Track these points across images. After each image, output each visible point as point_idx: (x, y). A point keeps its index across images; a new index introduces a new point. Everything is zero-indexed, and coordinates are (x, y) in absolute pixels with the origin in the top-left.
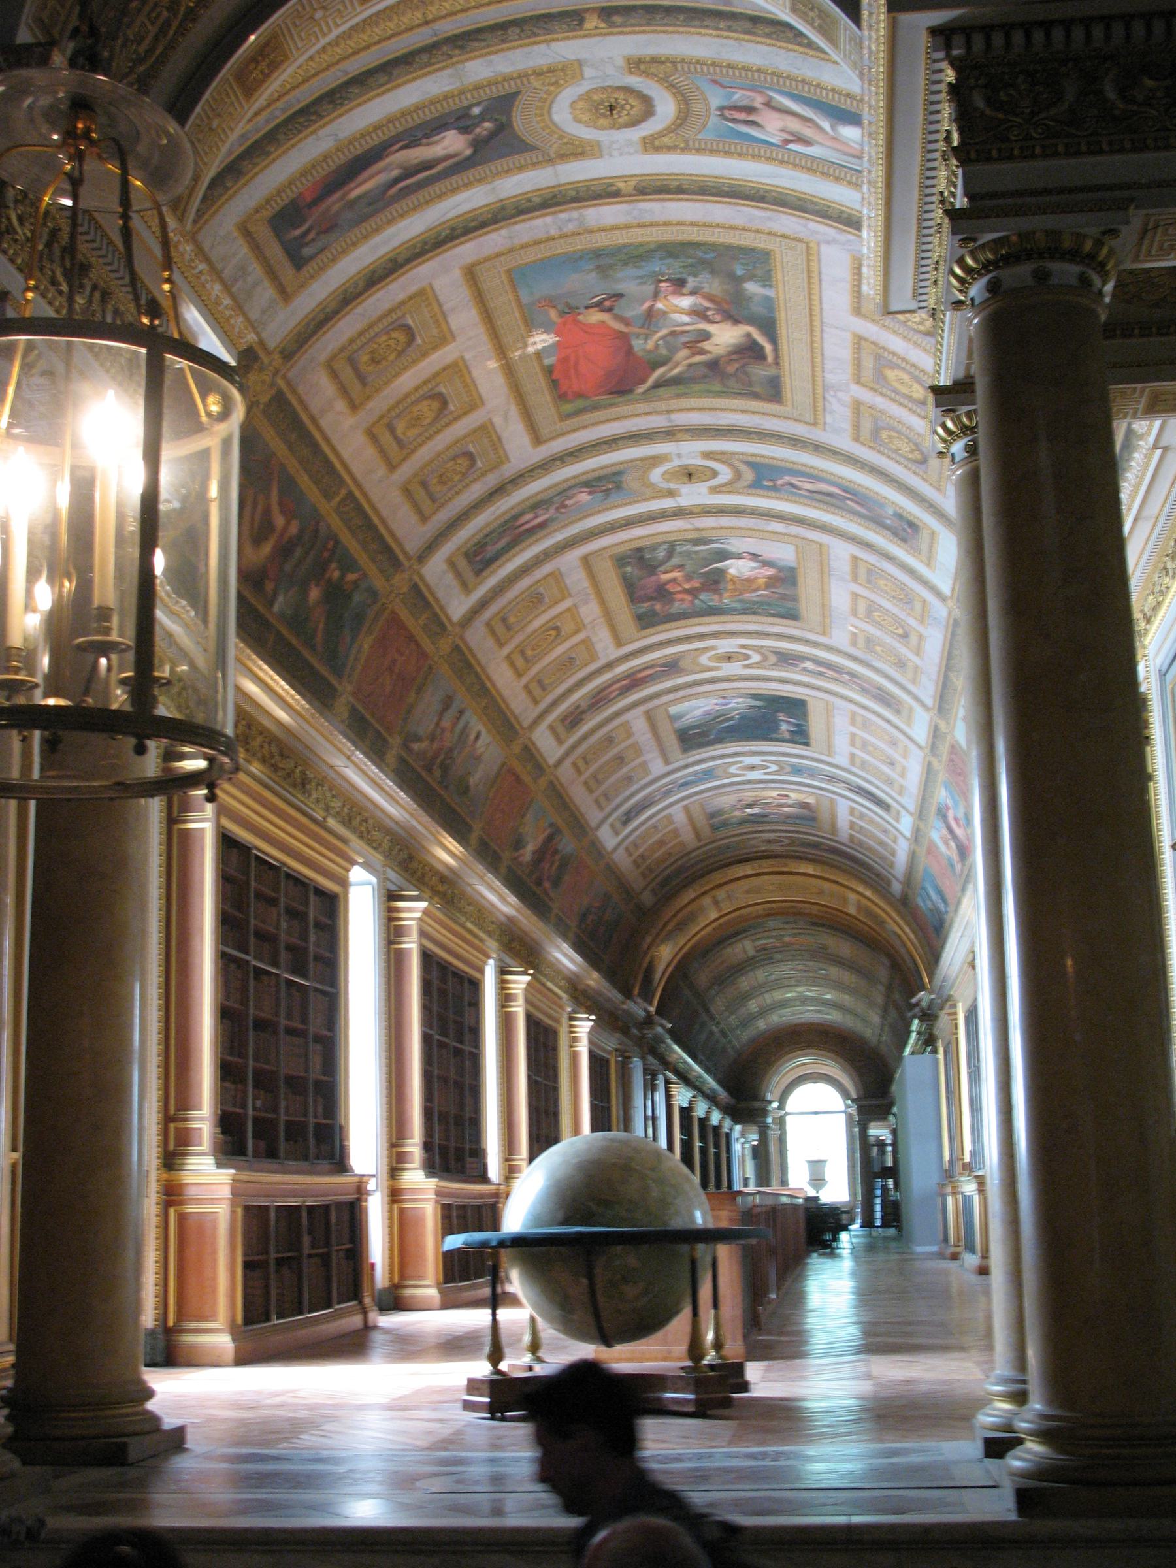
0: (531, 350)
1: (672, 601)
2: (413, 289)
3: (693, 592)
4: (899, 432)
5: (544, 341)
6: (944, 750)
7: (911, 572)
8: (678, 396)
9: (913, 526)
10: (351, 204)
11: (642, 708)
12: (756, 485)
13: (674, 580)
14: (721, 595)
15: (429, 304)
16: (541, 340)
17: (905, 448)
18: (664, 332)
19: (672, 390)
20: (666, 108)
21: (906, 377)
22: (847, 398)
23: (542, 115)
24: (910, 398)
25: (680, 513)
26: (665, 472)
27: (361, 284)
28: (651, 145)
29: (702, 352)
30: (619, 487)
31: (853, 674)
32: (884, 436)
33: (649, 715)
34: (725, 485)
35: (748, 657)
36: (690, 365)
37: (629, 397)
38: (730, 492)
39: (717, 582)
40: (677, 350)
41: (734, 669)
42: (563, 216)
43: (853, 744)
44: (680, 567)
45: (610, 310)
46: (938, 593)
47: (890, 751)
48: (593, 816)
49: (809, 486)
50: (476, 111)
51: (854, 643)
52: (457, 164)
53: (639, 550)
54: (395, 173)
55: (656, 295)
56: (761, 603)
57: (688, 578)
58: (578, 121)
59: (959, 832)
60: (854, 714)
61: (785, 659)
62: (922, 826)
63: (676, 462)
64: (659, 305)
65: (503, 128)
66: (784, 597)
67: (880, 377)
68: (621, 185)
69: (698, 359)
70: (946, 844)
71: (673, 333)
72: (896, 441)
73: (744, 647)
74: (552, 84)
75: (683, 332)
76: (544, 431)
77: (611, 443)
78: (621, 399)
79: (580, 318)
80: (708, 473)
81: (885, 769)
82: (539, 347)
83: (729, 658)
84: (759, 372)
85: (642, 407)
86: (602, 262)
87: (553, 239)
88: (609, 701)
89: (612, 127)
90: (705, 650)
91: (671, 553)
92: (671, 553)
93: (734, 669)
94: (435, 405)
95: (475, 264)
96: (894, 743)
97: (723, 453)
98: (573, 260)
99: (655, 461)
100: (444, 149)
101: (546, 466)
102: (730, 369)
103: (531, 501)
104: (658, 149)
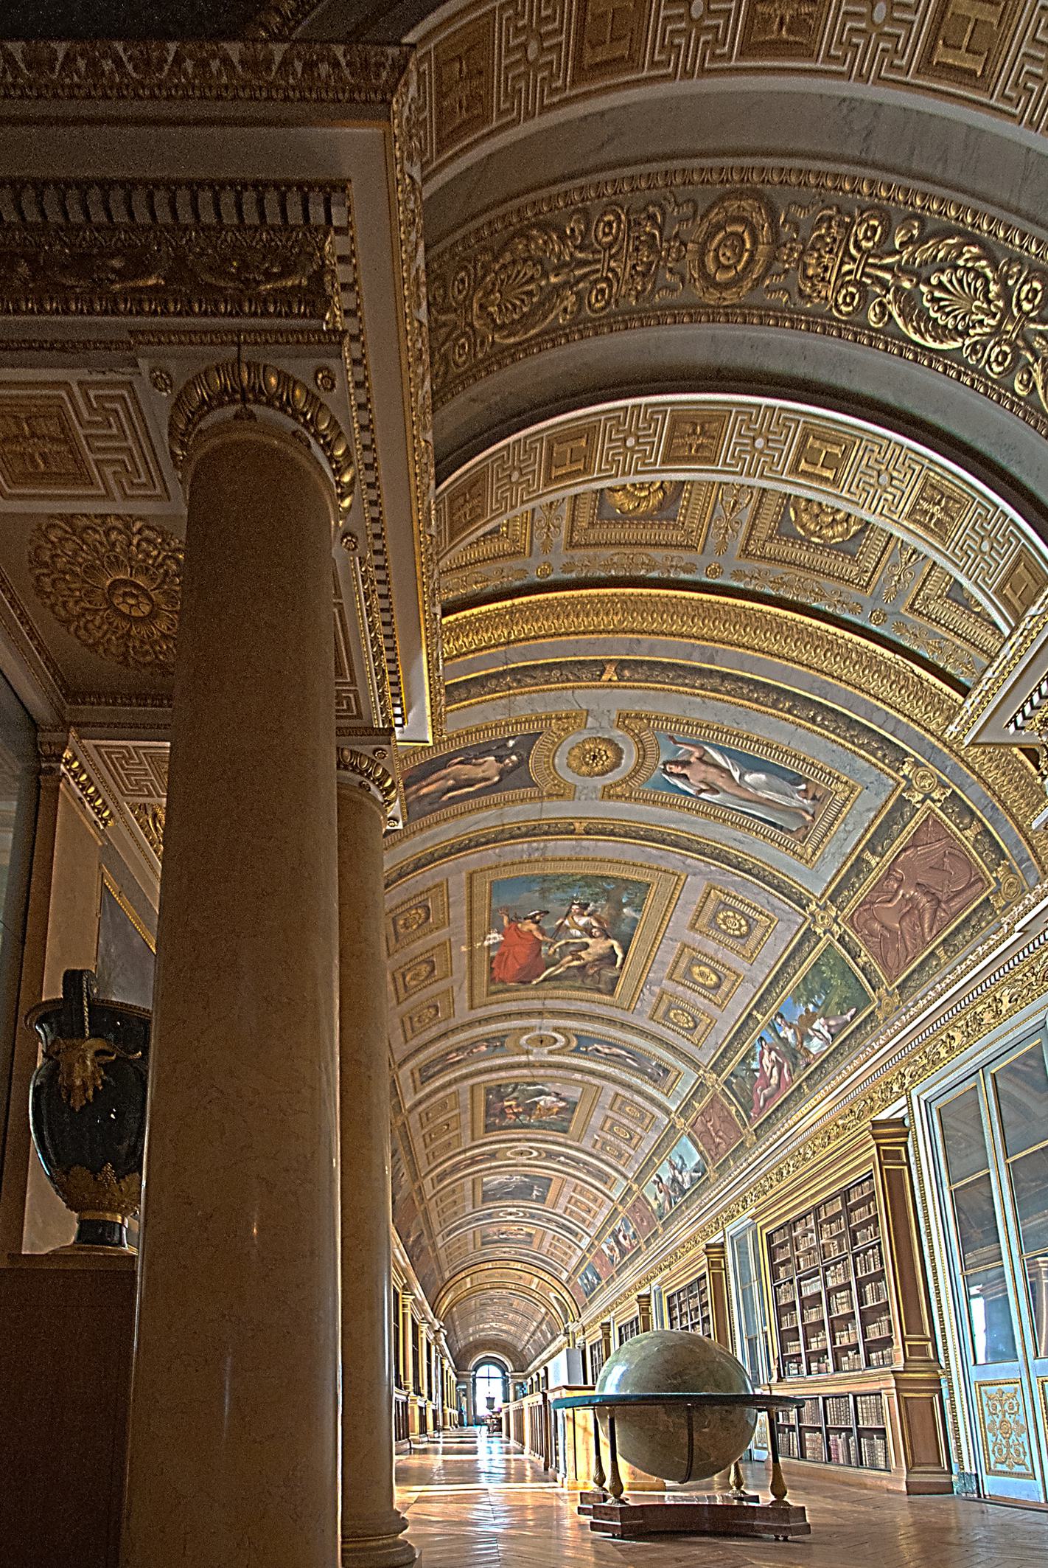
0: (486, 943)
1: (505, 1118)
2: (437, 880)
3: (517, 1114)
4: (683, 1010)
5: (495, 938)
6: (630, 1201)
7: (652, 1100)
8: (554, 988)
9: (666, 1071)
10: (421, 798)
11: (471, 1177)
12: (576, 1050)
13: (510, 1106)
14: (530, 1117)
15: (442, 896)
16: (495, 937)
17: (683, 1020)
18: (563, 942)
19: (553, 984)
20: (628, 762)
21: (707, 970)
22: (656, 989)
23: (549, 757)
24: (703, 986)
25: (527, 1065)
26: (529, 1039)
27: (412, 866)
28: (607, 793)
29: (579, 958)
30: (502, 1045)
31: (585, 1163)
32: (672, 1014)
33: (473, 1181)
34: (559, 1049)
35: (531, 1153)
36: (568, 968)
37: (530, 986)
38: (559, 1054)
39: (531, 1109)
40: (565, 956)
41: (523, 1159)
42: (535, 845)
43: (569, 1202)
44: (516, 1098)
45: (537, 923)
46: (668, 1112)
47: (591, 1205)
48: (437, 1228)
49: (607, 1051)
50: (511, 743)
51: (594, 1147)
52: (487, 787)
53: (500, 1086)
54: (451, 782)
55: (567, 915)
56: (550, 1123)
57: (518, 1106)
58: (569, 766)
59: (625, 1243)
60: (577, 1185)
61: (551, 1155)
62: (596, 1243)
63: (537, 1032)
64: (567, 922)
65: (523, 762)
66: (564, 1120)
67: (689, 971)
68: (577, 825)
69: (576, 963)
70: (612, 1249)
71: (567, 944)
72: (680, 1017)
73: (531, 1148)
74: (563, 730)
75: (574, 943)
76: (476, 1002)
77: (508, 1016)
78: (522, 987)
79: (519, 925)
80: (552, 1041)
81: (584, 1214)
82: (491, 942)
83: (521, 1153)
84: (607, 973)
85: (532, 993)
86: (546, 885)
87: (523, 863)
88: (461, 1170)
89: (589, 775)
90: (511, 1148)
91: (514, 1090)
92: (514, 1090)
93: (523, 1159)
94: (428, 969)
95: (475, 872)
96: (595, 1200)
97: (565, 1029)
98: (531, 880)
99: (526, 1030)
100: (483, 772)
101: (470, 1025)
102: (591, 972)
103: (456, 1047)
104: (610, 797)
